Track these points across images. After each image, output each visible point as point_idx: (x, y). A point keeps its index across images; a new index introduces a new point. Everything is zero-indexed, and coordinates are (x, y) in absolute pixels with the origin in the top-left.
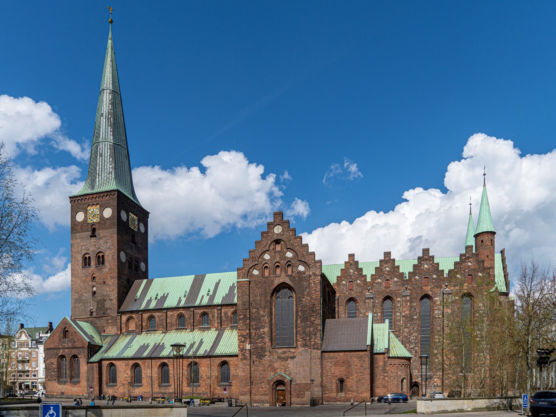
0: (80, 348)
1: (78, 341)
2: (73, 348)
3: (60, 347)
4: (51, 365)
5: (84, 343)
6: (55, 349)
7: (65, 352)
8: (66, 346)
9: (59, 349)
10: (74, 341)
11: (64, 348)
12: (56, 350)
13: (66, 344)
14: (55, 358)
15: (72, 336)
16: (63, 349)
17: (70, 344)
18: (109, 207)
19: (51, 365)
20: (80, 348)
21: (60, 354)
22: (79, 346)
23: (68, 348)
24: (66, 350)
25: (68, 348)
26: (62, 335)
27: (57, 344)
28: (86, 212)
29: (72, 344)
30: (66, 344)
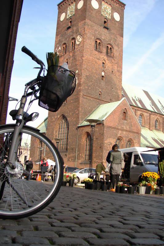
0: (135, 133)
1: (134, 126)
2: (130, 132)
3: (120, 128)
4: (109, 145)
5: (138, 129)
6: (114, 128)
7: (123, 134)
8: (125, 128)
9: (118, 129)
10: (131, 125)
11: (122, 130)
12: (115, 130)
13: (124, 127)
14: (114, 138)
15: (130, 119)
16: (121, 130)
17: (128, 128)
18: (119, 14)
19: (109, 145)
20: (135, 133)
21: (119, 135)
22: (135, 131)
23: (126, 131)
24: (124, 133)
25: (126, 131)
26: (122, 116)
27: (117, 124)
28: (100, 5)
29: (130, 128)
30: (124, 127)
